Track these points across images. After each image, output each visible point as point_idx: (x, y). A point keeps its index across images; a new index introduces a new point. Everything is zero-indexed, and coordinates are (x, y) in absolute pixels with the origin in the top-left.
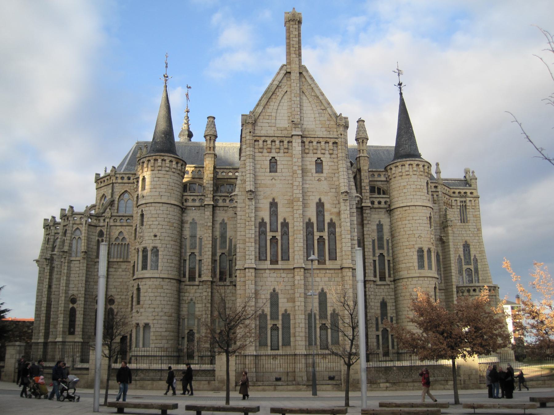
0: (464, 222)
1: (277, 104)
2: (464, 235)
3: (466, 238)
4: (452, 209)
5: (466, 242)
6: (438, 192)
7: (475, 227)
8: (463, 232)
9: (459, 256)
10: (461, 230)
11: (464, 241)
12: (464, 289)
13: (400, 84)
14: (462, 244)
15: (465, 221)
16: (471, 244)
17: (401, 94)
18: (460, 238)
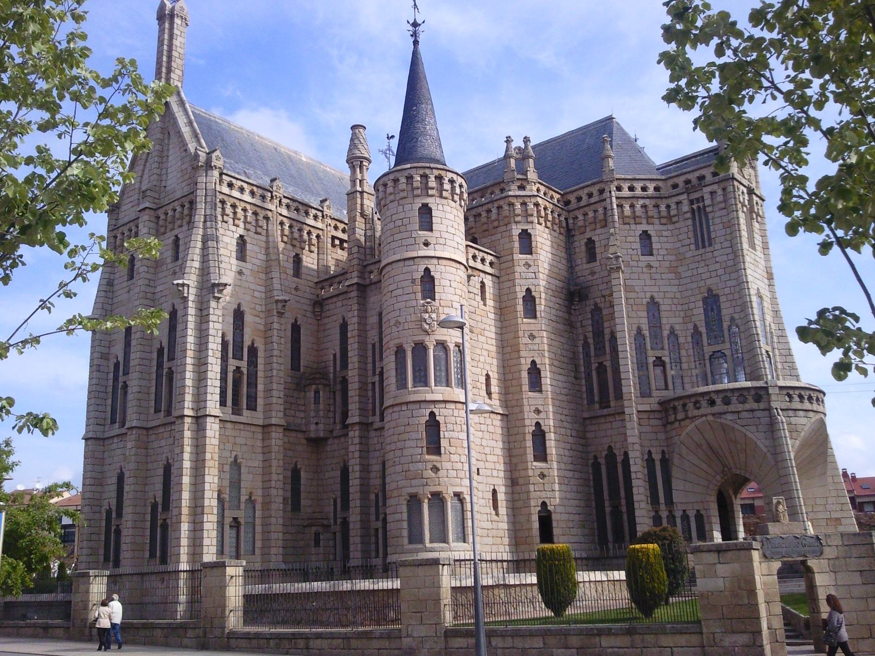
0: (704, 247)
1: (141, 167)
2: (704, 276)
3: (709, 282)
4: (674, 223)
5: (710, 290)
6: (605, 200)
7: (729, 251)
8: (700, 271)
9: (696, 327)
10: (696, 265)
11: (704, 290)
12: (676, 404)
13: (415, 25)
14: (699, 297)
15: (707, 243)
16: (720, 293)
17: (416, 43)
18: (694, 285)
